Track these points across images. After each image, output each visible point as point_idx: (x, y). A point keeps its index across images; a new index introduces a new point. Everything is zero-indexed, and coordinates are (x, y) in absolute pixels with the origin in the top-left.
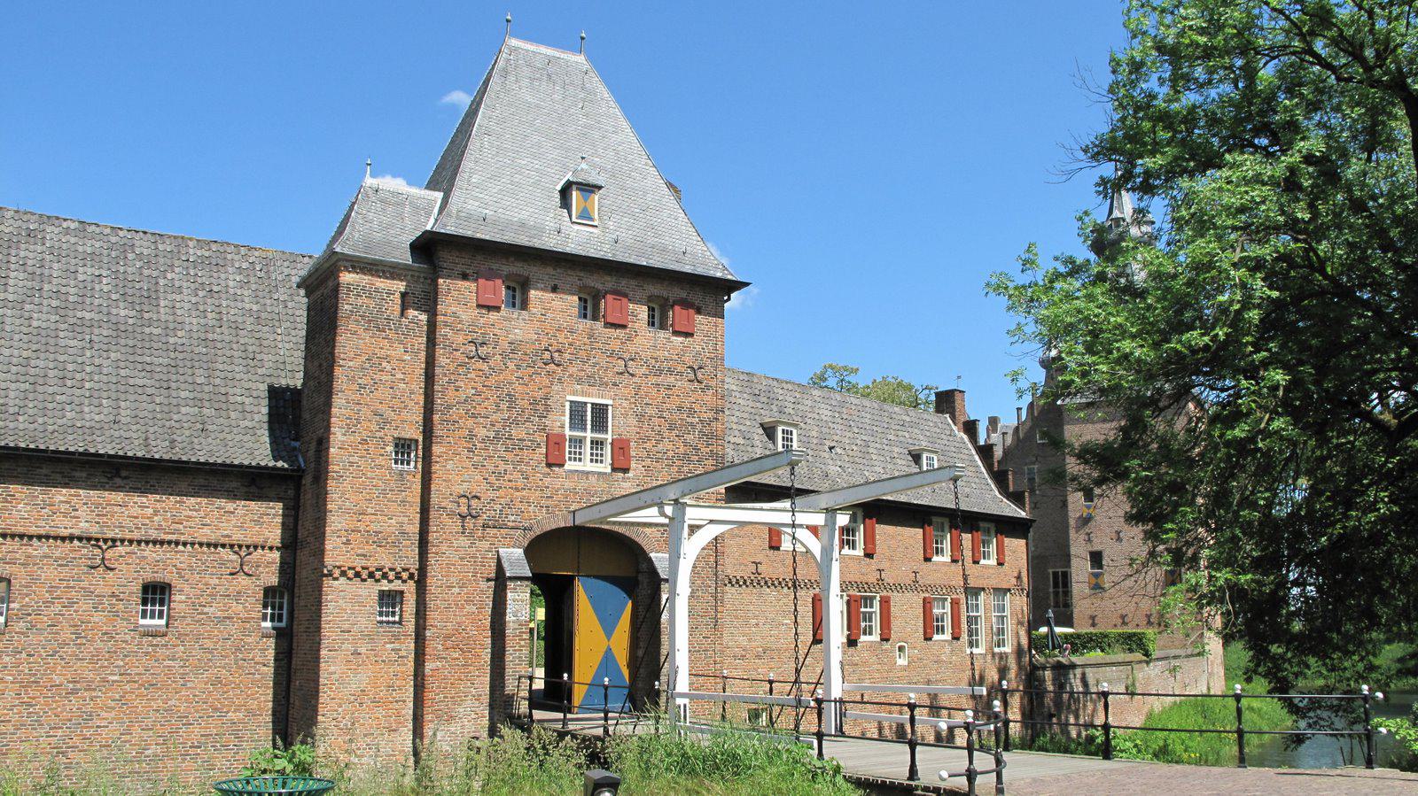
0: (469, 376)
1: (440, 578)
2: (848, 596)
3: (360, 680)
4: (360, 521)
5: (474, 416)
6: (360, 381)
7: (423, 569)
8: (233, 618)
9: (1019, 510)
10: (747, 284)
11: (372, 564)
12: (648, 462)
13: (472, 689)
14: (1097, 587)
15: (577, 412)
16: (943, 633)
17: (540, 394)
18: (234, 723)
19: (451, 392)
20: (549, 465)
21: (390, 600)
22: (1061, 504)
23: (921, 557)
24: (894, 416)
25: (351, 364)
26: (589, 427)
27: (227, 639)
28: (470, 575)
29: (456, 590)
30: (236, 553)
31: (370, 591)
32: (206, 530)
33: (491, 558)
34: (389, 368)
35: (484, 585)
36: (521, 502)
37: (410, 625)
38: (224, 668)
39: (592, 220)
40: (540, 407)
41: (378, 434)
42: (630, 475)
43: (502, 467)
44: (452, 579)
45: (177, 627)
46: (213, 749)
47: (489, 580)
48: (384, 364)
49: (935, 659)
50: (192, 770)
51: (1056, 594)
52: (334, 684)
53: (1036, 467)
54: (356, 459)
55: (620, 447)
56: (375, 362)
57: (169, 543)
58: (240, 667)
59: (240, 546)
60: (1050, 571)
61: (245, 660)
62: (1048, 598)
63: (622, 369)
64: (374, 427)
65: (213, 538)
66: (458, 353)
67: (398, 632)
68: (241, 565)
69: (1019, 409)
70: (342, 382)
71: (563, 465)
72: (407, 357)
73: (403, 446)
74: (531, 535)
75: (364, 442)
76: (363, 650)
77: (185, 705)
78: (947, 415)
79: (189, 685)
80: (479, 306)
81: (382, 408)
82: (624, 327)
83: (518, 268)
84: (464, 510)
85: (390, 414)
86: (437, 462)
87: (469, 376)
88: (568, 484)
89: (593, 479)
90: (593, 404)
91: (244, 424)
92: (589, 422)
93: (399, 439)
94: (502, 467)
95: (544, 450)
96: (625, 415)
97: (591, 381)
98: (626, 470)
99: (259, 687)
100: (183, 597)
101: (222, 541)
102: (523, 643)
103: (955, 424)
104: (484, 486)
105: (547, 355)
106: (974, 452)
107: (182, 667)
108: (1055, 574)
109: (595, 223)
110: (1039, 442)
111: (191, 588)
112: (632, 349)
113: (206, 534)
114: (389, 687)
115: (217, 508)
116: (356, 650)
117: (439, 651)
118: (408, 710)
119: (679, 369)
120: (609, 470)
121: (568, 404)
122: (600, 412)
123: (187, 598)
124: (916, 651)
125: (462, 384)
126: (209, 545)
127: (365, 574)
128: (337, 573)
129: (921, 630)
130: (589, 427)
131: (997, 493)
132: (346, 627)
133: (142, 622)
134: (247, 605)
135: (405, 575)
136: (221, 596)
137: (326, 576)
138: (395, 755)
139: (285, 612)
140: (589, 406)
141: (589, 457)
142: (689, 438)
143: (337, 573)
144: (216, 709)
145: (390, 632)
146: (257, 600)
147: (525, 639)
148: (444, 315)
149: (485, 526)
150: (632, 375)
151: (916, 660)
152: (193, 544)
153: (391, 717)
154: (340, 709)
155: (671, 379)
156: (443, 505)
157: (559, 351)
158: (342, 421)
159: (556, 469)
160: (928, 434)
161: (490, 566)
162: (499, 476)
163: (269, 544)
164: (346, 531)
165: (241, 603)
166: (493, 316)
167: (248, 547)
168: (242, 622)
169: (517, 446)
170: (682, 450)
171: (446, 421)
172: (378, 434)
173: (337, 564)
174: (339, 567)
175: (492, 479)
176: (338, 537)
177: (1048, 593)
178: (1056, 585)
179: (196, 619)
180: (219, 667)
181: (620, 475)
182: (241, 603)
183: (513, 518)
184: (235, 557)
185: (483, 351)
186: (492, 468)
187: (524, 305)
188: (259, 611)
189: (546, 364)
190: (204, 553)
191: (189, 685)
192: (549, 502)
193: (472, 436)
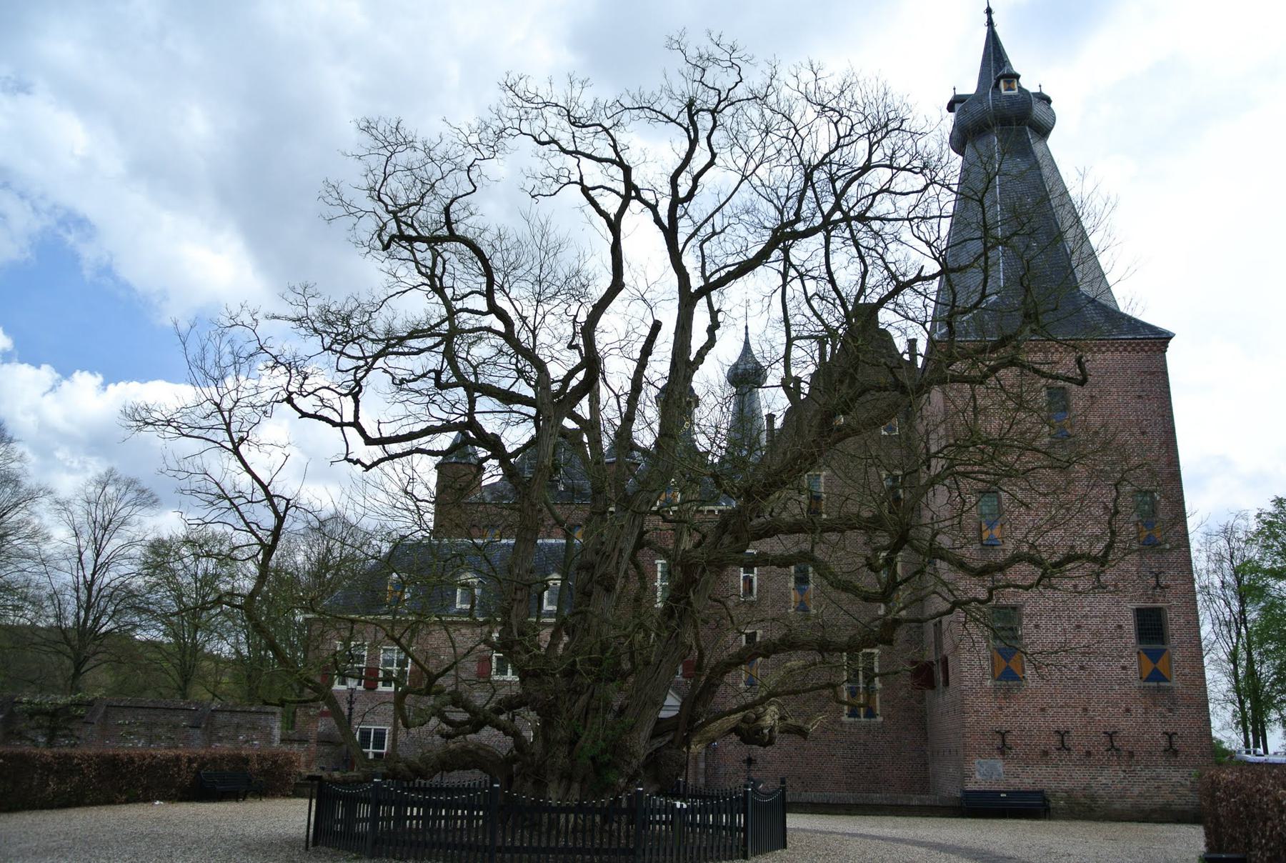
14: (1008, 677)
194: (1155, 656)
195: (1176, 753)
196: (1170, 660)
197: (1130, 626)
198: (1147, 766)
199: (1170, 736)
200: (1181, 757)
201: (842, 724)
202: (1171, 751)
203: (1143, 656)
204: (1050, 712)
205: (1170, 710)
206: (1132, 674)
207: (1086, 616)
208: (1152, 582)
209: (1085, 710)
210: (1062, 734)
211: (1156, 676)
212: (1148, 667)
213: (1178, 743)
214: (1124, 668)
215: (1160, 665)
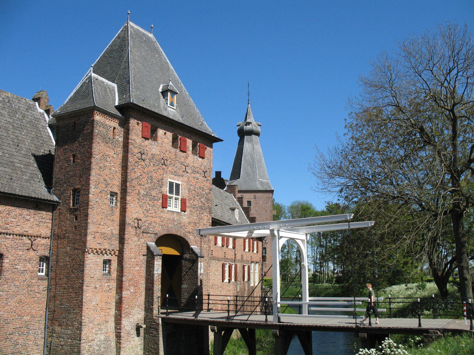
0: (139, 167)
1: (128, 254)
2: (229, 264)
3: (97, 299)
4: (98, 228)
5: (140, 185)
6: (100, 165)
7: (121, 251)
8: (27, 271)
10: (222, 141)
11: (103, 247)
12: (191, 209)
13: (137, 303)
15: (171, 184)
17: (160, 177)
18: (26, 322)
19: (133, 174)
20: (163, 207)
21: (107, 262)
25: (97, 157)
26: (174, 193)
27: (24, 281)
28: (138, 253)
29: (133, 260)
30: (30, 239)
31: (100, 260)
32: (18, 228)
33: (145, 246)
34: (109, 160)
35: (142, 257)
36: (154, 223)
37: (114, 275)
38: (23, 295)
39: (174, 106)
40: (160, 183)
41: (106, 190)
42: (186, 213)
43: (148, 207)
44: (133, 255)
45: (5, 275)
46: (18, 335)
47: (144, 255)
48: (108, 158)
50: (9, 346)
52: (88, 302)
54: (98, 200)
55: (183, 202)
56: (105, 157)
57: (4, 234)
58: (29, 294)
59: (31, 236)
61: (31, 291)
63: (184, 170)
64: (104, 186)
65: (21, 232)
66: (135, 157)
67: (109, 278)
68: (32, 245)
70: (94, 165)
71: (166, 208)
72: (115, 156)
73: (113, 194)
74: (157, 237)
75: (101, 192)
76: (98, 286)
77: (7, 314)
78: (232, 194)
79: (9, 304)
80: (142, 137)
81: (107, 178)
82: (185, 152)
83: (155, 123)
84: (136, 225)
85: (109, 181)
86: (128, 204)
87: (139, 167)
88: (168, 216)
89: (175, 214)
90: (176, 183)
91: (24, 177)
92: (174, 191)
93: (111, 192)
94: (148, 207)
95: (161, 201)
96: (185, 189)
97: (176, 174)
98: (185, 211)
99: (36, 304)
100: (8, 261)
101: (25, 233)
102: (159, 283)
103: (235, 198)
104: (143, 215)
105: (162, 161)
106: (241, 209)
107: (7, 295)
109: (175, 108)
111: (12, 256)
112: (187, 162)
113: (18, 230)
114: (106, 302)
115: (23, 218)
116: (95, 286)
117: (127, 286)
118: (113, 312)
119: (200, 171)
120: (179, 211)
121: (168, 182)
122: (178, 186)
123: (10, 261)
125: (136, 170)
126: (19, 235)
127: (100, 251)
128: (90, 251)
130: (174, 193)
132: (92, 276)
133: (39, 274)
134: (33, 264)
135: (112, 253)
136: (23, 260)
137: (86, 252)
138: (107, 333)
139: (44, 268)
140: (174, 184)
141: (174, 205)
142: (202, 200)
143: (90, 251)
144: (19, 315)
145: (107, 278)
146: (37, 262)
147: (160, 281)
148: (131, 140)
149: (143, 232)
150: (187, 172)
152: (13, 235)
153: (106, 316)
154: (90, 313)
155: (198, 175)
156: (130, 222)
157: (166, 160)
158: (94, 182)
159: (165, 209)
161: (144, 250)
162: (148, 211)
163: (42, 236)
164: (94, 232)
165: (31, 264)
166: (147, 142)
167: (34, 237)
168: (31, 273)
169: (153, 199)
170: (200, 205)
171: (131, 186)
172: (106, 190)
173: (91, 247)
174: (91, 248)
175: (145, 212)
176: (92, 235)
179: (13, 271)
180: (21, 295)
181: (183, 213)
182: (31, 264)
183: (151, 229)
184: (29, 242)
185: (144, 157)
186: (145, 208)
187: (155, 139)
188: (38, 268)
189: (162, 165)
190: (17, 239)
191: (9, 304)
192: (163, 223)
193: (139, 193)
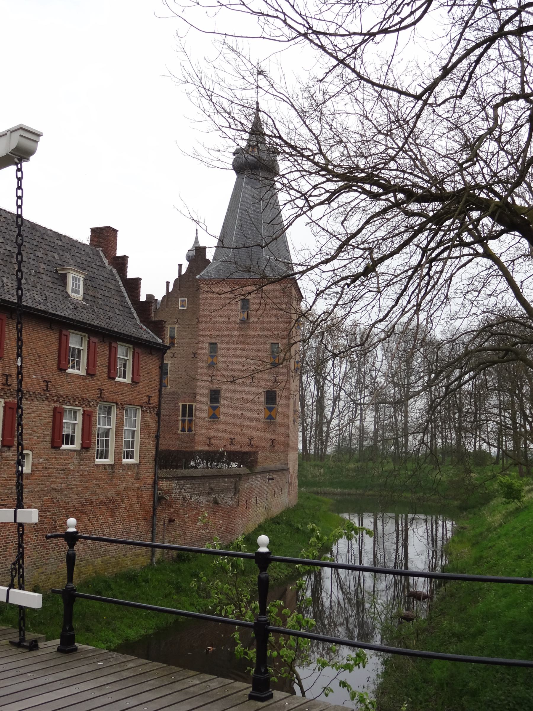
9: (156, 337)
14: (214, 416)
16: (73, 443)
22: (192, 356)
23: (55, 367)
24: (46, 237)
49: (62, 468)
51: (183, 421)
53: (176, 326)
60: (181, 404)
62: (178, 424)
69: (168, 283)
108: (184, 407)
110: (180, 308)
124: (41, 460)
129: (49, 439)
131: (138, 322)
151: (40, 468)
160: (79, 260)
177: (178, 420)
178: (184, 415)
194: (270, 409)
195: (274, 446)
196: (277, 412)
197: (263, 397)
198: (262, 452)
199: (273, 440)
200: (276, 448)
201: (178, 434)
202: (273, 446)
203: (266, 410)
204: (228, 431)
205: (274, 431)
206: (261, 417)
207: (246, 394)
208: (273, 379)
209: (242, 430)
210: (232, 439)
211: (270, 417)
212: (268, 413)
213: (275, 443)
214: (258, 414)
215: (273, 413)
